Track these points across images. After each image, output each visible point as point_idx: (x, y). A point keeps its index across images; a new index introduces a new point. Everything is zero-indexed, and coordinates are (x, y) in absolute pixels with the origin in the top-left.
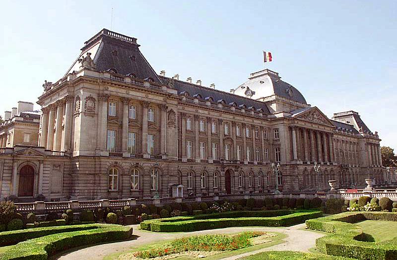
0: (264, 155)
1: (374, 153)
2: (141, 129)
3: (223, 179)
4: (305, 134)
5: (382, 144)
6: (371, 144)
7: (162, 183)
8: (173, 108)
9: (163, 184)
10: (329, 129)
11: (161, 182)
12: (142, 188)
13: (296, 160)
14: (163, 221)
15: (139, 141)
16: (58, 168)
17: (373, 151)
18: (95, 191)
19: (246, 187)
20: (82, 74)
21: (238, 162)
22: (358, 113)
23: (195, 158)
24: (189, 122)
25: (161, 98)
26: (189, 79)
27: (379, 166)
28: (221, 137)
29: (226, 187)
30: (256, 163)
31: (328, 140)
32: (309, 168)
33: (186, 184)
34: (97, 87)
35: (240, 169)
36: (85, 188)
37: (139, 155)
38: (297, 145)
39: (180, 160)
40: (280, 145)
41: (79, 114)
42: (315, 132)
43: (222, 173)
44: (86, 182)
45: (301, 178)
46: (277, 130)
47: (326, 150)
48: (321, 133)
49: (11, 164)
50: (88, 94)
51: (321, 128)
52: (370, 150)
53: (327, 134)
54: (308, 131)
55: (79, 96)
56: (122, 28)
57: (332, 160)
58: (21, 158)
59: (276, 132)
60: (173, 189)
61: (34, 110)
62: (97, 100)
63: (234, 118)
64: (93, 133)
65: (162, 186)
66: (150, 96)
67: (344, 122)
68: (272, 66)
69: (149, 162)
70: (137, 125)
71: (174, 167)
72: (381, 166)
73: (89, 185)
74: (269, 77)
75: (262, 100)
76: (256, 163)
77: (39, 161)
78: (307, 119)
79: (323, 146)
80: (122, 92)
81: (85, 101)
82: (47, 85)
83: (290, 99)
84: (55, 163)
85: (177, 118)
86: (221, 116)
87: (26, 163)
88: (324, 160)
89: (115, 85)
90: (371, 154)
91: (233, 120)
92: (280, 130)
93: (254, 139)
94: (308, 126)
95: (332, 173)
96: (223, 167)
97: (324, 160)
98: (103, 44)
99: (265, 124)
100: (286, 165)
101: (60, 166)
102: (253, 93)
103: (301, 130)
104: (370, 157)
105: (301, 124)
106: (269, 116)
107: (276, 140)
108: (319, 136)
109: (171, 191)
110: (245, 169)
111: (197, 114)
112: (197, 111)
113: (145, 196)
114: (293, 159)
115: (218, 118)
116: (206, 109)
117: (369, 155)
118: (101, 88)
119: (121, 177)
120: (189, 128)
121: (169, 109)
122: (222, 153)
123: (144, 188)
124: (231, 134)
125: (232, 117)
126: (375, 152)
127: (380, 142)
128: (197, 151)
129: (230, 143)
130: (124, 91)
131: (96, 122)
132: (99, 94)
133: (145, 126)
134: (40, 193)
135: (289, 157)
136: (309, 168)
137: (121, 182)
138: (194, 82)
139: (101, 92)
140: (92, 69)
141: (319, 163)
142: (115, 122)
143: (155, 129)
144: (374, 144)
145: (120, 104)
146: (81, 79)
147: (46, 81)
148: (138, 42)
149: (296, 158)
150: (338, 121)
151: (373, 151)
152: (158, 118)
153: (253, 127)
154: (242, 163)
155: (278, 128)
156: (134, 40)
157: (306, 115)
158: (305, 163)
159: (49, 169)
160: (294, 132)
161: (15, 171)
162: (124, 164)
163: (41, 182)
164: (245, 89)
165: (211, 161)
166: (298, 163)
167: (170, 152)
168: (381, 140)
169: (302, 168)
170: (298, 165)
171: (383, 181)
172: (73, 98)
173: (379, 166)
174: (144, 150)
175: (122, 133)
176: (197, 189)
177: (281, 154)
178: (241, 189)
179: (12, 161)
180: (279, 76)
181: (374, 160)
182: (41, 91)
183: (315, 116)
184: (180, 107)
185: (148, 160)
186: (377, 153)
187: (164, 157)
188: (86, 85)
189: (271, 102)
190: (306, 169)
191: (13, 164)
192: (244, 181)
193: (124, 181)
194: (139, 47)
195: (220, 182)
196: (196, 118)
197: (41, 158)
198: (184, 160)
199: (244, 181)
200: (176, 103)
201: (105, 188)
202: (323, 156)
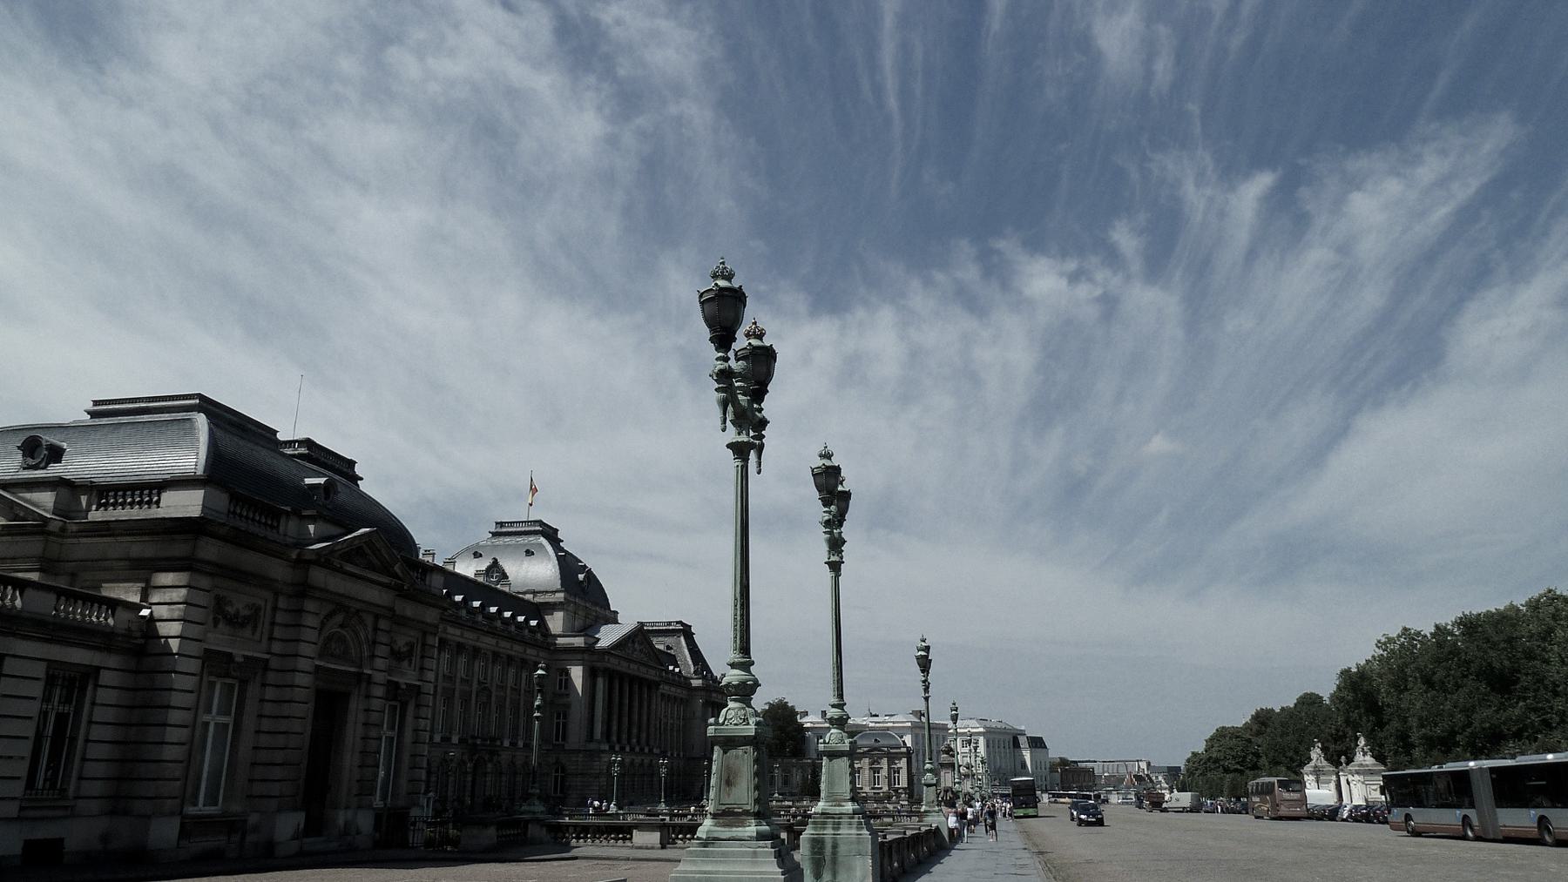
13: (599, 742)
28: (475, 686)
30: (521, 744)
31: (650, 697)
40: (568, 706)
53: (652, 685)
67: (661, 647)
75: (529, 597)
103: (611, 675)
105: (613, 663)
107: (561, 695)
110: (505, 757)
125: (493, 641)
141: (632, 749)
160: (600, 681)
165: (455, 739)
189: (551, 607)
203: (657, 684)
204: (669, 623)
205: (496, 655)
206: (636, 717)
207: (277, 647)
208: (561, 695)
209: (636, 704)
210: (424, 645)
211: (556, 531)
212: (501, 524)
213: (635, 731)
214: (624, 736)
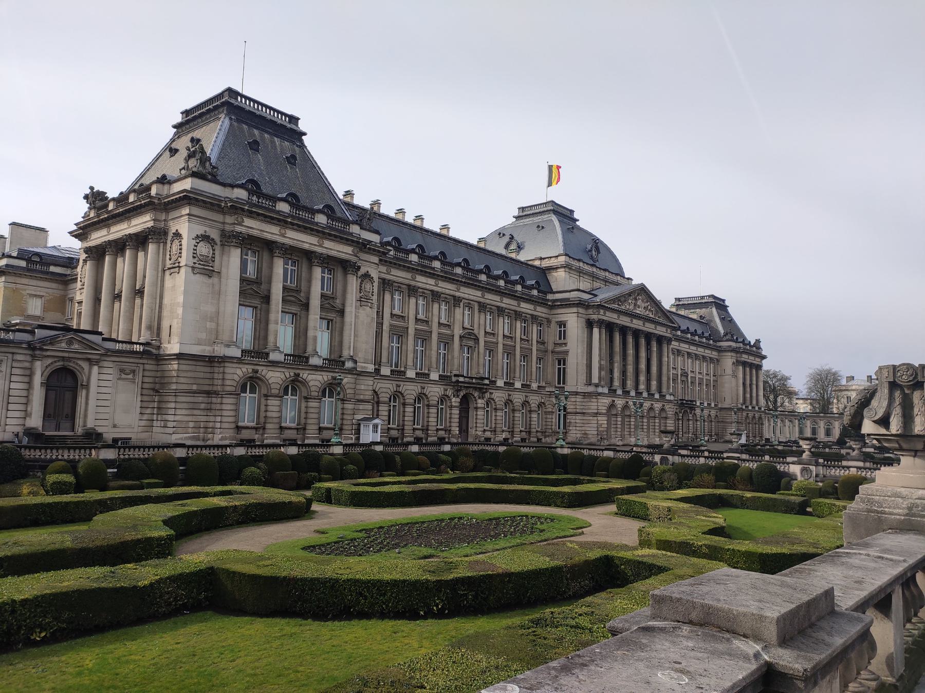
0: (534, 369)
1: (748, 382)
2: (306, 306)
3: (456, 411)
4: (617, 337)
5: (766, 365)
6: (744, 364)
7: (343, 414)
8: (369, 269)
9: (345, 417)
10: (664, 329)
11: (340, 412)
12: (303, 421)
13: (597, 386)
14: (355, 485)
15: (301, 335)
16: (130, 376)
17: (748, 377)
18: (211, 425)
19: (498, 429)
20: (187, 184)
21: (487, 382)
23: (405, 368)
24: (397, 297)
25: (349, 249)
26: (401, 211)
27: (757, 408)
28: (458, 332)
29: (460, 427)
30: (518, 385)
32: (620, 403)
33: (386, 418)
34: (219, 217)
35: (487, 395)
36: (190, 418)
37: (300, 358)
38: (600, 355)
39: (377, 371)
40: (566, 352)
41: (179, 267)
42: (637, 333)
43: (454, 399)
44: (191, 406)
45: (603, 420)
46: (562, 324)
47: (654, 369)
48: (649, 336)
49: (27, 365)
50: (200, 230)
51: (649, 328)
52: (741, 375)
53: (660, 340)
54: (624, 330)
55: (181, 232)
56: (269, 91)
57: (664, 390)
58: (48, 353)
59: (560, 327)
60: (362, 426)
61: (50, 244)
62: (219, 243)
63: (483, 297)
64: (210, 309)
65: (342, 419)
66: (327, 244)
67: (694, 316)
68: (561, 195)
69: (320, 373)
70: (297, 301)
71: (366, 386)
72: (760, 408)
73: (196, 412)
74: (554, 218)
75: (537, 263)
76: (518, 385)
77: (89, 360)
78: (623, 307)
79: (649, 361)
80: (271, 232)
81: (194, 242)
82: (96, 198)
83: (592, 265)
85: (376, 290)
86: (458, 290)
87: (61, 363)
88: (648, 388)
89: (258, 214)
90: (744, 384)
91: (482, 300)
92: (569, 325)
93: (518, 340)
94: (624, 321)
95: (664, 415)
96: (457, 387)
97: (648, 388)
98: (227, 121)
99: (541, 311)
100: (577, 393)
101: (134, 372)
102: (520, 248)
103: (610, 327)
104: (741, 388)
105: (611, 317)
106: (550, 297)
107: (560, 345)
108: (643, 341)
109: (358, 432)
110: (499, 396)
111: (413, 283)
112: (414, 279)
113: (308, 438)
114: (589, 383)
115: (452, 293)
116: (432, 275)
117: (737, 386)
118: (229, 219)
119: (263, 400)
120: (396, 311)
121: (363, 270)
122: (456, 361)
123: (309, 421)
124: (476, 326)
125: (479, 293)
126: (751, 380)
127: (764, 362)
129: (471, 343)
130: (275, 229)
131: (217, 288)
132: (223, 231)
133: (315, 302)
134: (90, 424)
135: (583, 378)
136: (620, 403)
137: (263, 408)
138: (409, 218)
139: (228, 228)
140: (210, 177)
142: (254, 292)
143: (334, 310)
144: (751, 366)
145: (266, 256)
146: (187, 198)
147: (92, 188)
148: (302, 126)
149: (595, 380)
150: (682, 312)
151: (748, 377)
152: (339, 287)
153: (518, 315)
154: (494, 382)
155: (566, 321)
156: (294, 120)
157: (623, 299)
158: (612, 391)
160: (596, 331)
161: (38, 379)
162: (270, 374)
163: (92, 403)
164: (506, 239)
165: (434, 376)
166: (600, 390)
167: (360, 355)
168: (764, 357)
169: (607, 401)
170: (600, 394)
171: (761, 437)
172: (166, 233)
173: (757, 408)
174: (310, 349)
175: (268, 312)
176: (406, 427)
177: (568, 371)
178: (488, 434)
179: (29, 358)
180: (576, 216)
181: (748, 396)
182: (80, 210)
183: (639, 302)
184: (383, 269)
185: (316, 368)
186: (754, 382)
187: (349, 365)
188: (197, 211)
190: (612, 406)
191: (32, 362)
192: (494, 418)
193: (270, 408)
194: (304, 137)
195: (450, 418)
196: (412, 291)
197: (94, 354)
198: (385, 371)
199: (494, 418)
200: (375, 259)
201: (232, 419)
202: (648, 380)
203: (669, 341)
204: (702, 297)
205: (483, 307)
206: (643, 366)
208: (560, 345)
209: (643, 354)
211: (572, 212)
212: (522, 209)
213: (642, 378)
214: (630, 383)
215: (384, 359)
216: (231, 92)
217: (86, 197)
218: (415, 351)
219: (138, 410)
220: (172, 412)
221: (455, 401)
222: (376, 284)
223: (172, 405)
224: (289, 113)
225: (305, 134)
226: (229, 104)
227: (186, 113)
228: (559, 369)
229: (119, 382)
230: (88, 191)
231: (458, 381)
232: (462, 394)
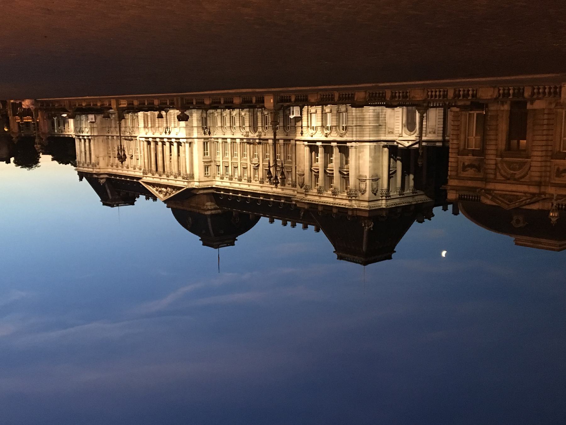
22: (104, 204)
29: (257, 116)
52: (93, 156)
84: (392, 135)
128: (282, 151)
159: (396, 129)
166: (185, 140)
204: (118, 206)
207: (548, 164)
210: (457, 171)
215: (294, 147)
216: (365, 263)
217: (433, 216)
218: (280, 153)
219: (387, 116)
220: (370, 116)
221: (260, 129)
222: (297, 182)
223: (371, 119)
224: (342, 261)
225: (334, 252)
226: (367, 259)
227: (390, 258)
228: (207, 150)
229: (392, 127)
230: (432, 218)
231: (259, 139)
232: (257, 134)
